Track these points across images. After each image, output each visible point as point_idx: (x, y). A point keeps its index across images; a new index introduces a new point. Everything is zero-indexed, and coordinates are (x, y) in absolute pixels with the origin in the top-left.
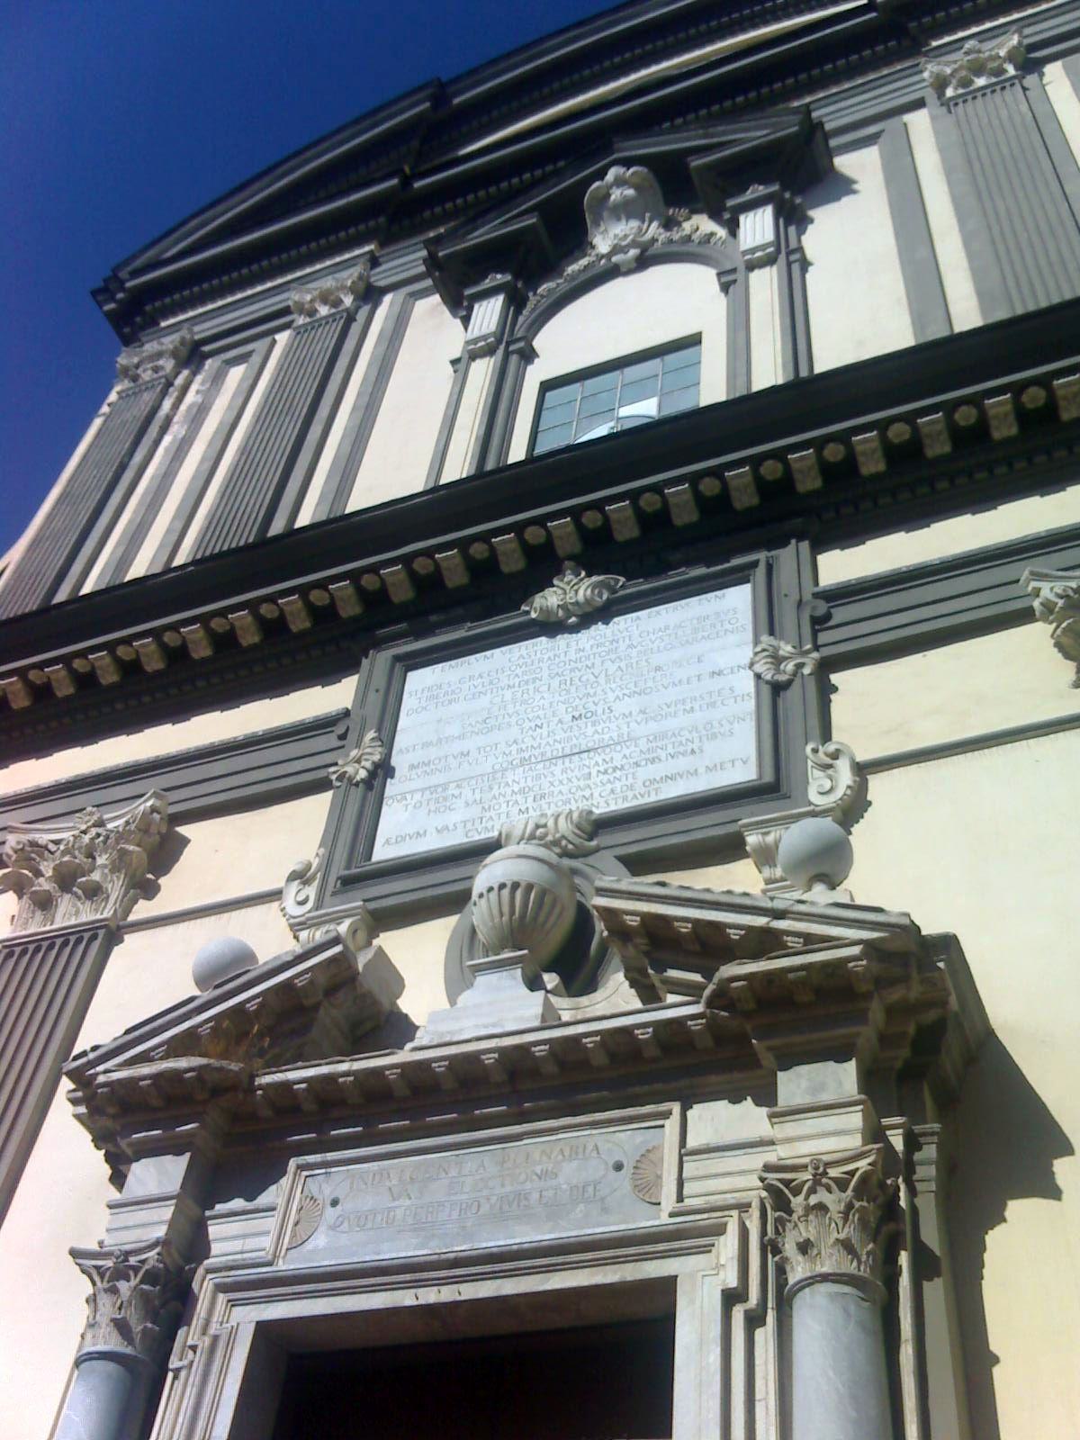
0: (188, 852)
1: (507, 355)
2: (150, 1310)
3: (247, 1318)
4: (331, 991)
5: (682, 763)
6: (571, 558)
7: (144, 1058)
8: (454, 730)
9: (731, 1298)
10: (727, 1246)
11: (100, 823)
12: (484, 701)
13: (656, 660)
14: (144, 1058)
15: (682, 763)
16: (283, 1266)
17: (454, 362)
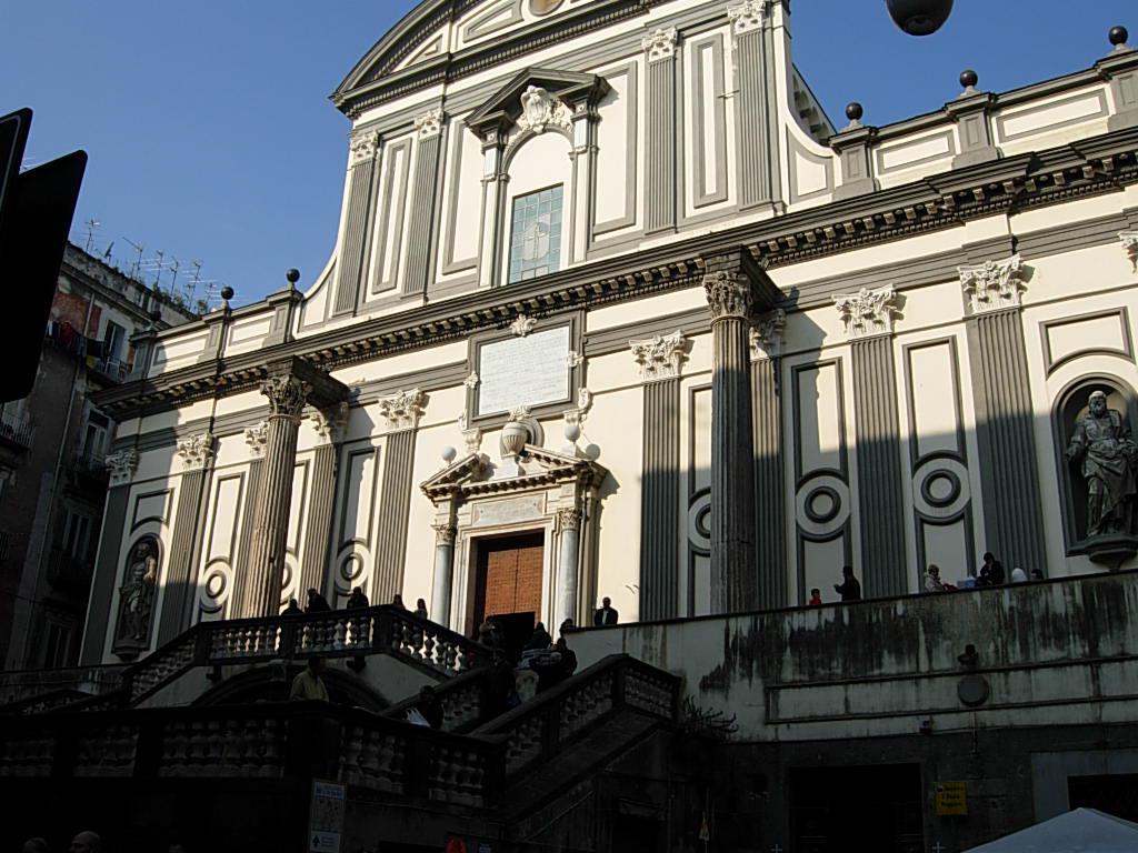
0: (430, 400)
1: (500, 181)
2: (449, 535)
3: (469, 536)
4: (474, 465)
5: (552, 389)
6: (521, 312)
7: (436, 484)
8: (495, 371)
9: (553, 532)
10: (553, 521)
11: (404, 395)
12: (502, 361)
13: (546, 352)
14: (436, 484)
15: (552, 389)
16: (474, 526)
17: (482, 181)
